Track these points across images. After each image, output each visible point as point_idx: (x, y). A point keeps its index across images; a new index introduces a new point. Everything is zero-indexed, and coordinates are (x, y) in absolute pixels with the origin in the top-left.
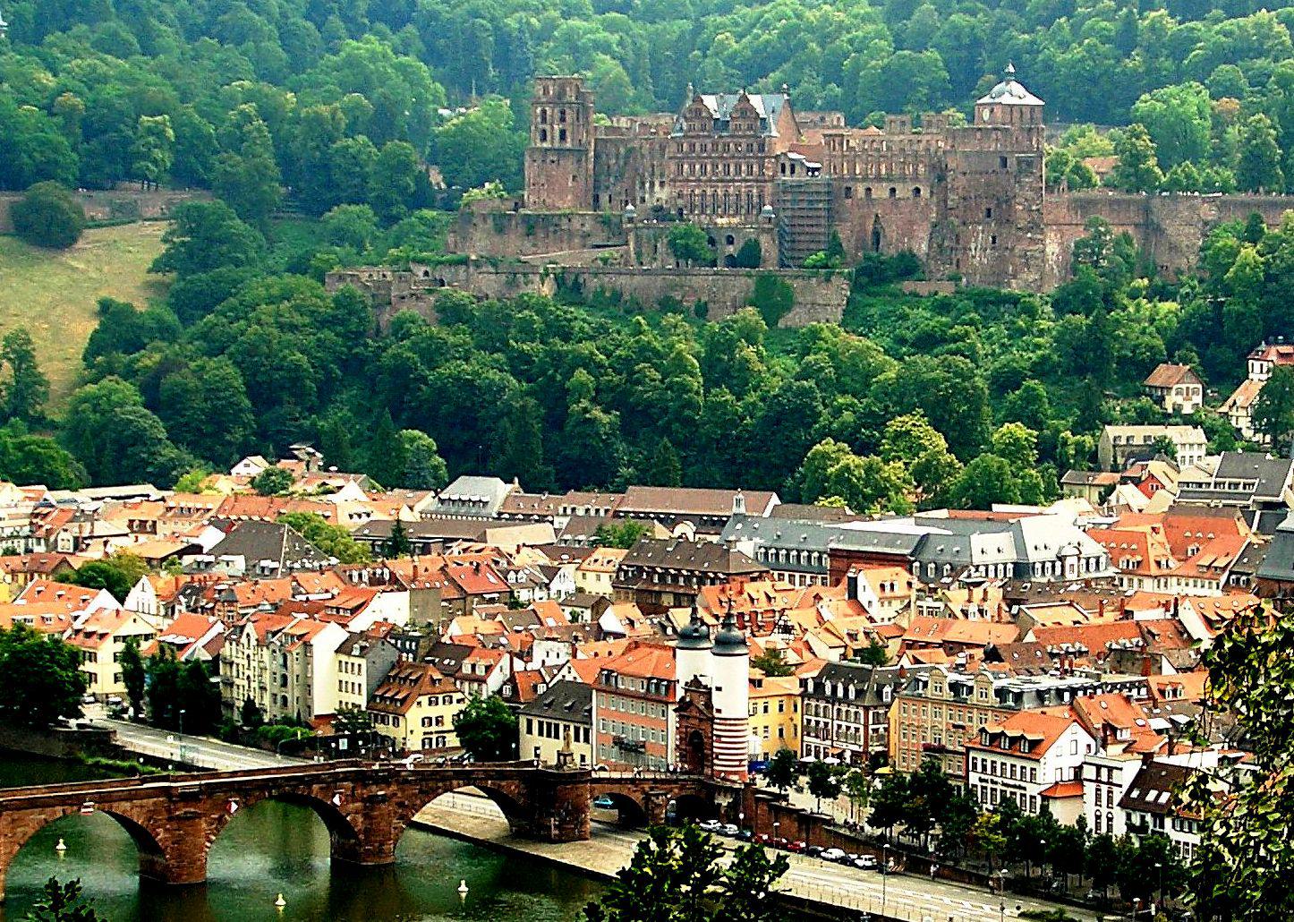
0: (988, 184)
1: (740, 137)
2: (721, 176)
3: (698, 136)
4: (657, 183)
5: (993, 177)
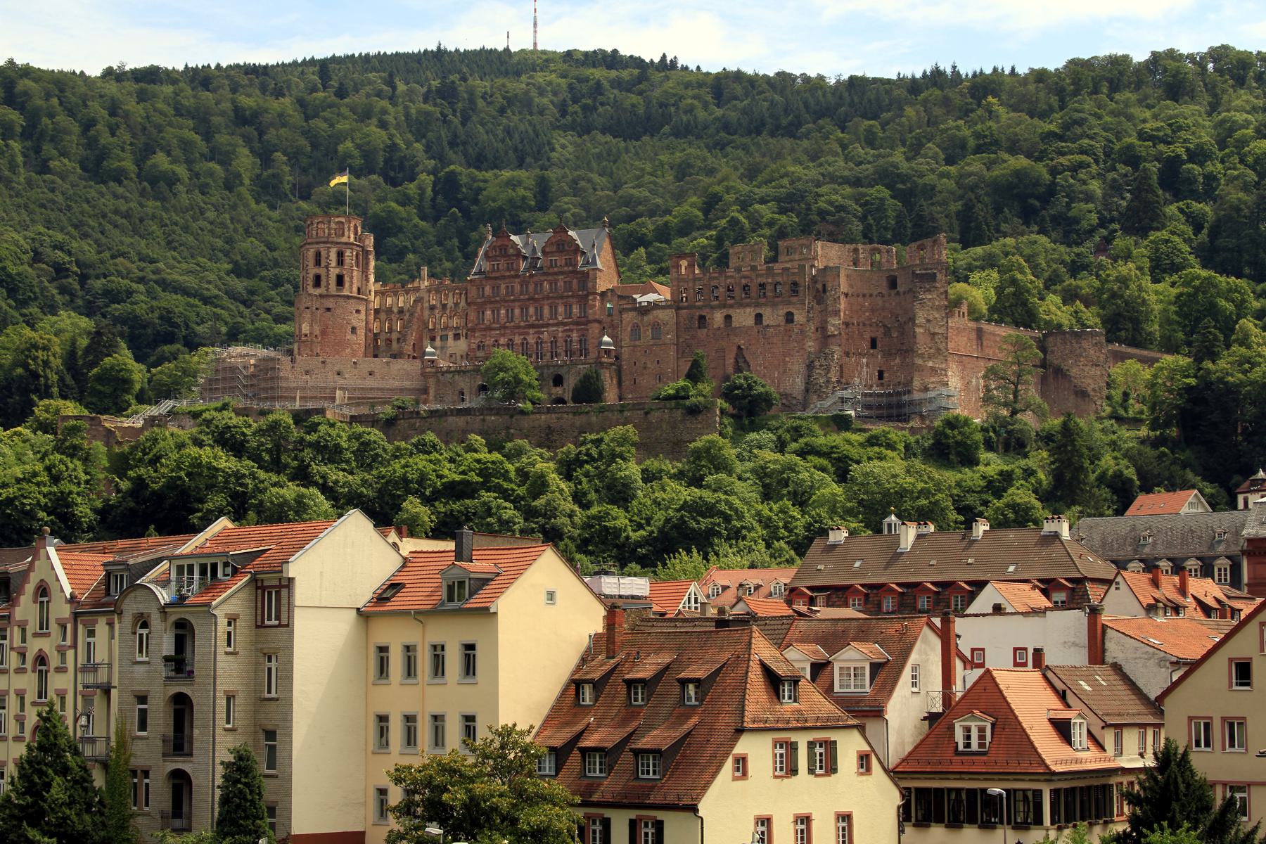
1: (556, 274)
2: (532, 320)
3: (504, 277)
4: (451, 334)
5: (880, 301)
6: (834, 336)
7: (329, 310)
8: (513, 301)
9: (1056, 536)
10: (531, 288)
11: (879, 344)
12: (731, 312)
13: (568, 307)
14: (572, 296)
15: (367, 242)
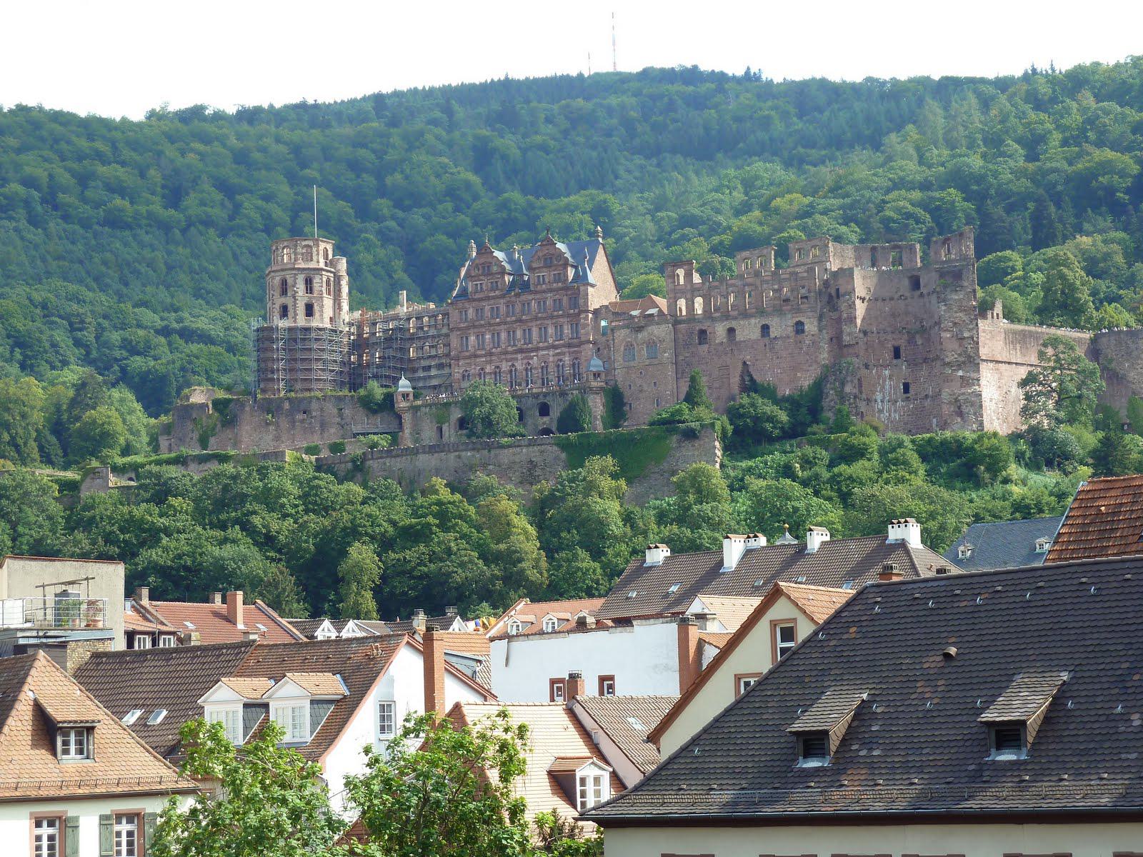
0: (893, 315)
1: (544, 292)
3: (488, 298)
5: (902, 304)
6: (849, 346)
8: (499, 324)
9: (902, 545)
10: (518, 308)
11: (903, 354)
12: (734, 324)
13: (559, 328)
14: (562, 316)
15: (339, 267)
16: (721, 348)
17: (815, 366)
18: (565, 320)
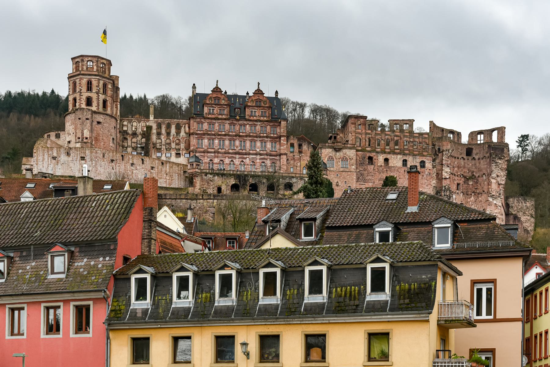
1: (256, 121)
5: (462, 162)
6: (446, 178)
7: (99, 123)
8: (225, 135)
12: (388, 156)
16: (381, 169)
17: (429, 186)
18: (269, 139)
